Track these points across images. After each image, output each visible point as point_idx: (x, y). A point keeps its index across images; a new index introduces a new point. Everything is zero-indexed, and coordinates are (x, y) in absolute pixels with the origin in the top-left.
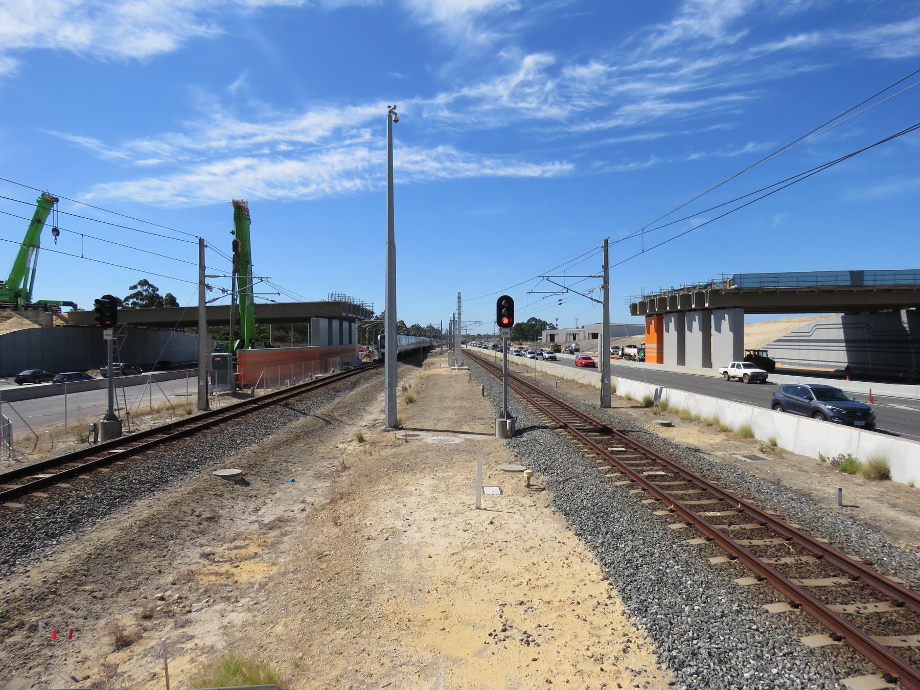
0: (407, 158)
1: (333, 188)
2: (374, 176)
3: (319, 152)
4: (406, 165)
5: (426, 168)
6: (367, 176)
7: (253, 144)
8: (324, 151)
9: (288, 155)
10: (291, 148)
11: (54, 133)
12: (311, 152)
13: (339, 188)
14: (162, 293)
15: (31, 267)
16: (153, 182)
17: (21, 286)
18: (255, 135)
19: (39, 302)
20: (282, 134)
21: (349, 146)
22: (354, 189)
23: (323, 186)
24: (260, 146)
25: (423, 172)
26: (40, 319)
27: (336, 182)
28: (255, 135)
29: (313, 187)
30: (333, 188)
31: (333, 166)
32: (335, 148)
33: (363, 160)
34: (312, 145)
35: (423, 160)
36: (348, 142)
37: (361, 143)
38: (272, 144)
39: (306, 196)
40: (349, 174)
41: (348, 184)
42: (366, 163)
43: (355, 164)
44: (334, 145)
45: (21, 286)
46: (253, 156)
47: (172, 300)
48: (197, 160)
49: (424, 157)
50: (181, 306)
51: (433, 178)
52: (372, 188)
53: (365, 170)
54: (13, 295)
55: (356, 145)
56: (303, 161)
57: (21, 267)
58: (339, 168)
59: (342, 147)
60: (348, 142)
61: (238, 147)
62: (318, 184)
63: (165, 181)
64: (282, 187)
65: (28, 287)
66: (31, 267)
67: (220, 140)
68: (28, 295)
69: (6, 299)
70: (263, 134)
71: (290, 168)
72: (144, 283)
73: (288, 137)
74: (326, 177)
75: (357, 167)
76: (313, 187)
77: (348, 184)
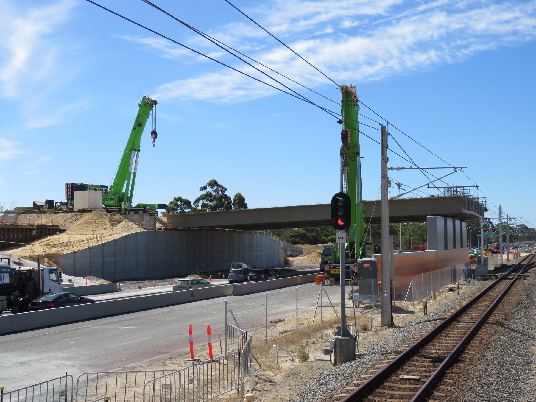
0: (495, 18)
1: (402, 64)
2: (452, 44)
3: (389, 23)
4: (494, 27)
5: (519, 28)
6: (444, 46)
7: (316, 24)
8: (394, 22)
9: (353, 32)
10: (356, 23)
11: (128, 38)
12: (379, 25)
13: (409, 64)
14: (231, 194)
15: (133, 171)
16: (214, 77)
17: (124, 190)
18: (318, 13)
19: (139, 206)
20: (347, 8)
21: (423, 12)
22: (428, 62)
23: (391, 63)
24: (322, 25)
25: (515, 33)
26: (145, 222)
27: (407, 57)
28: (318, 13)
29: (380, 65)
30: (402, 64)
31: (403, 38)
32: (407, 17)
33: (440, 26)
34: (380, 17)
35: (516, 18)
36: (422, 8)
37: (437, 7)
38: (335, 22)
39: (372, 76)
40: (422, 46)
41: (421, 58)
42: (443, 30)
43: (429, 33)
44: (405, 13)
45: (124, 190)
46: (314, 38)
47: (240, 200)
48: (258, 48)
49: (517, 14)
50: (250, 207)
51: (528, 39)
52: (449, 60)
53: (442, 38)
54: (117, 199)
55: (432, 10)
56: (369, 36)
57: (125, 172)
58: (410, 40)
59: (416, 15)
60: (422, 8)
61: (299, 29)
62: (385, 62)
63: (225, 74)
64: (346, 69)
65: (129, 192)
66: (133, 171)
67: (281, 24)
68: (129, 201)
69: (111, 203)
70: (326, 12)
71: (356, 46)
72: (214, 183)
73: (353, 12)
74: (395, 52)
75: (432, 36)
76: (380, 65)
77: (421, 58)
